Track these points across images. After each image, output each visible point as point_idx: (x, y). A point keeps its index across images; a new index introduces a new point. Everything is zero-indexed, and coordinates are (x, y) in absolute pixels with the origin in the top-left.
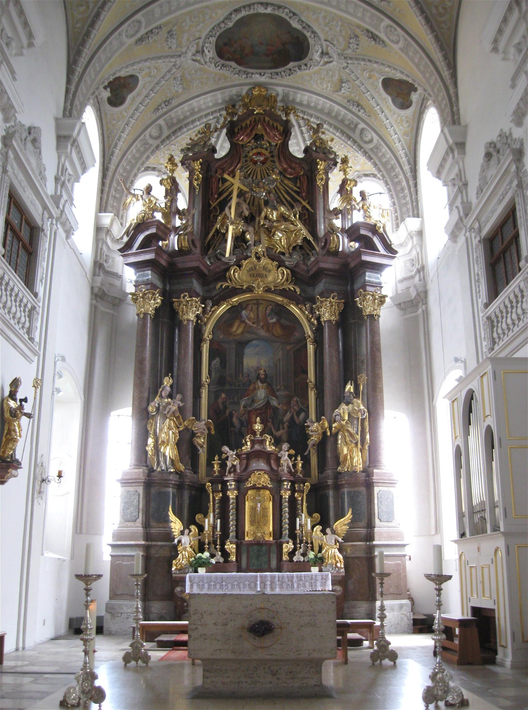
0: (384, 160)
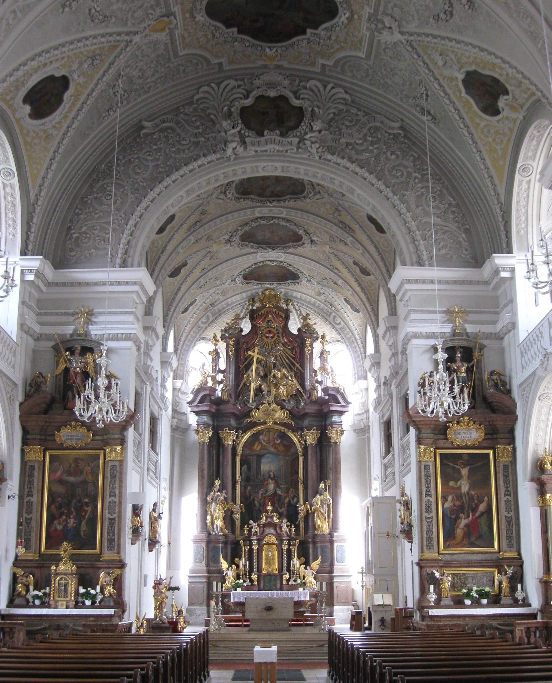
0: (348, 336)
